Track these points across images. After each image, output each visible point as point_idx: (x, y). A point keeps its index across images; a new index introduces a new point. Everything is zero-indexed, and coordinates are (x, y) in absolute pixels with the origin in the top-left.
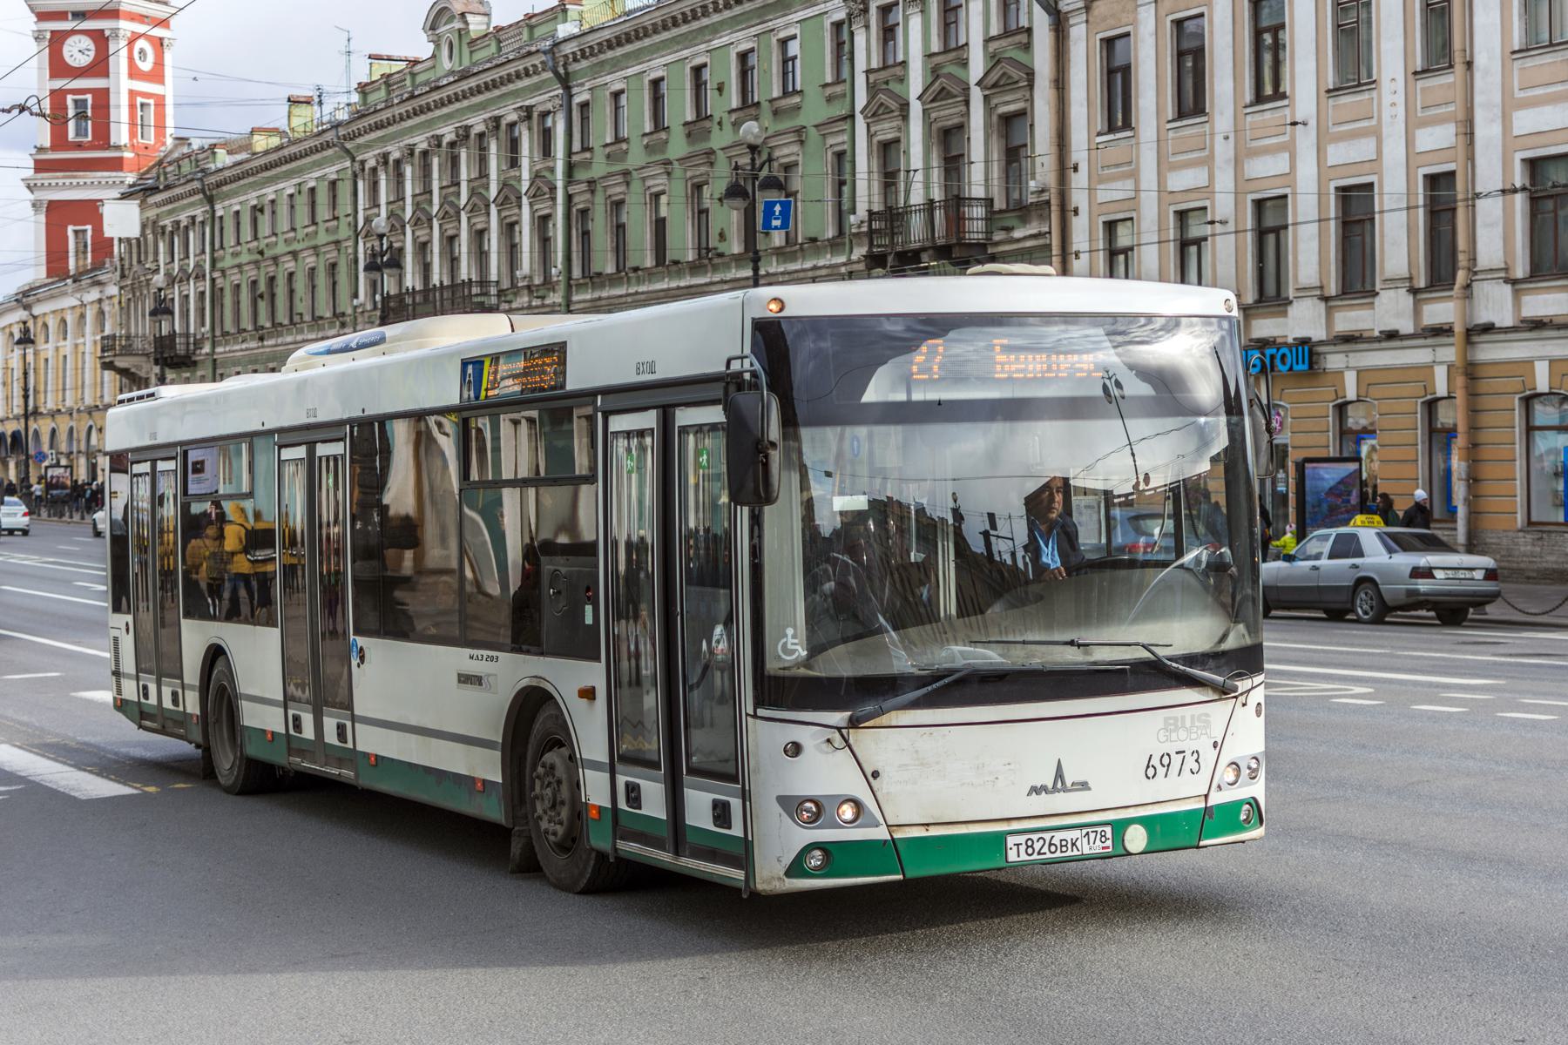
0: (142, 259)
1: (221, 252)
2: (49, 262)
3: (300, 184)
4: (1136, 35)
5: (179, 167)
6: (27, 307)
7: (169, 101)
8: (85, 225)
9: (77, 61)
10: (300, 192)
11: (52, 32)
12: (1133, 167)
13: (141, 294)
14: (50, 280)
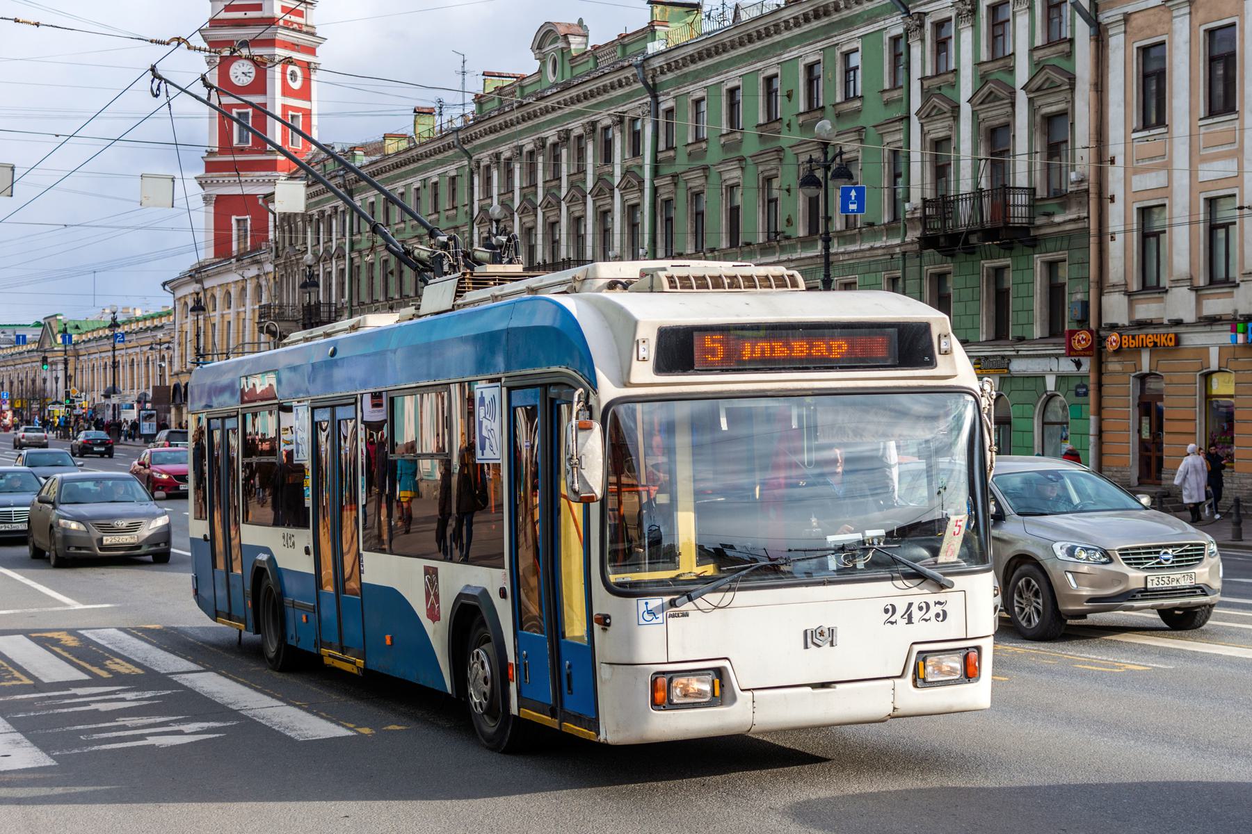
0: (293, 242)
1: (358, 237)
2: (216, 245)
3: (425, 180)
4: (1171, 43)
5: (325, 166)
6: (199, 281)
7: (314, 111)
9: (241, 81)
10: (425, 187)
12: (1166, 159)
13: (292, 271)
14: (217, 260)
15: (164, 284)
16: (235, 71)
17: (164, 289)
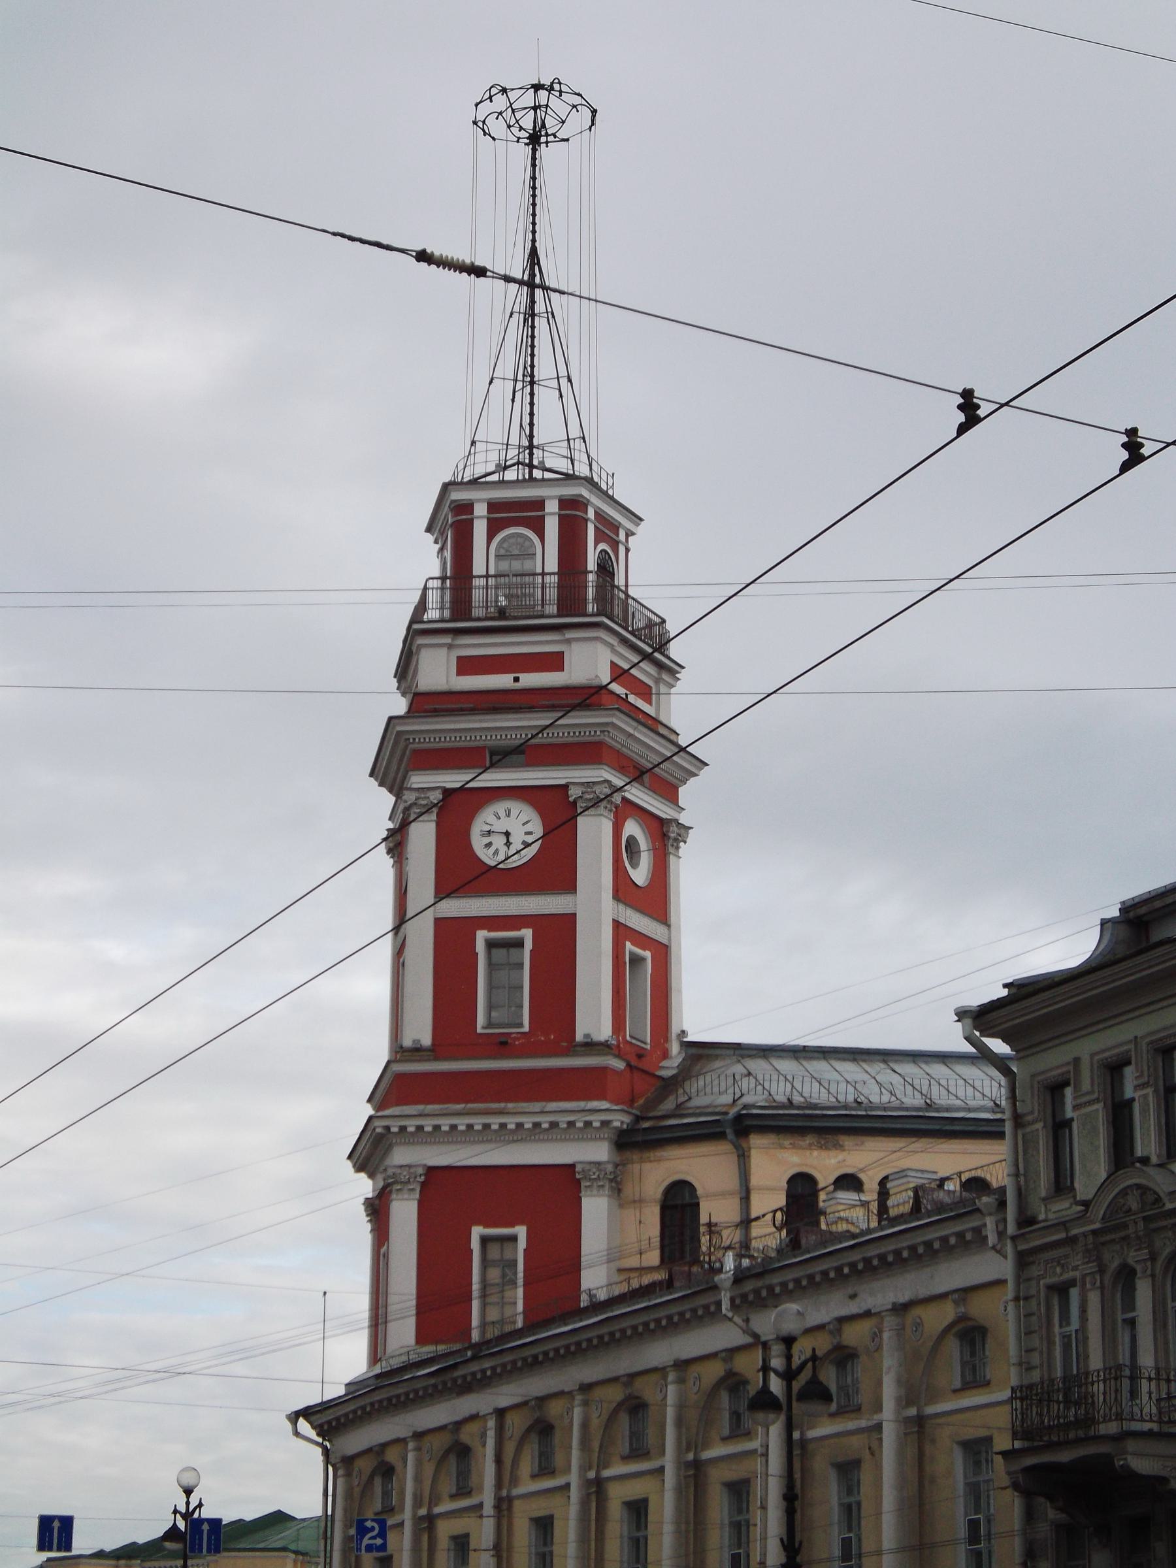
2: (419, 1314)
8: (512, 1225)
14: (428, 1350)
15: (294, 1417)
17: (297, 1433)
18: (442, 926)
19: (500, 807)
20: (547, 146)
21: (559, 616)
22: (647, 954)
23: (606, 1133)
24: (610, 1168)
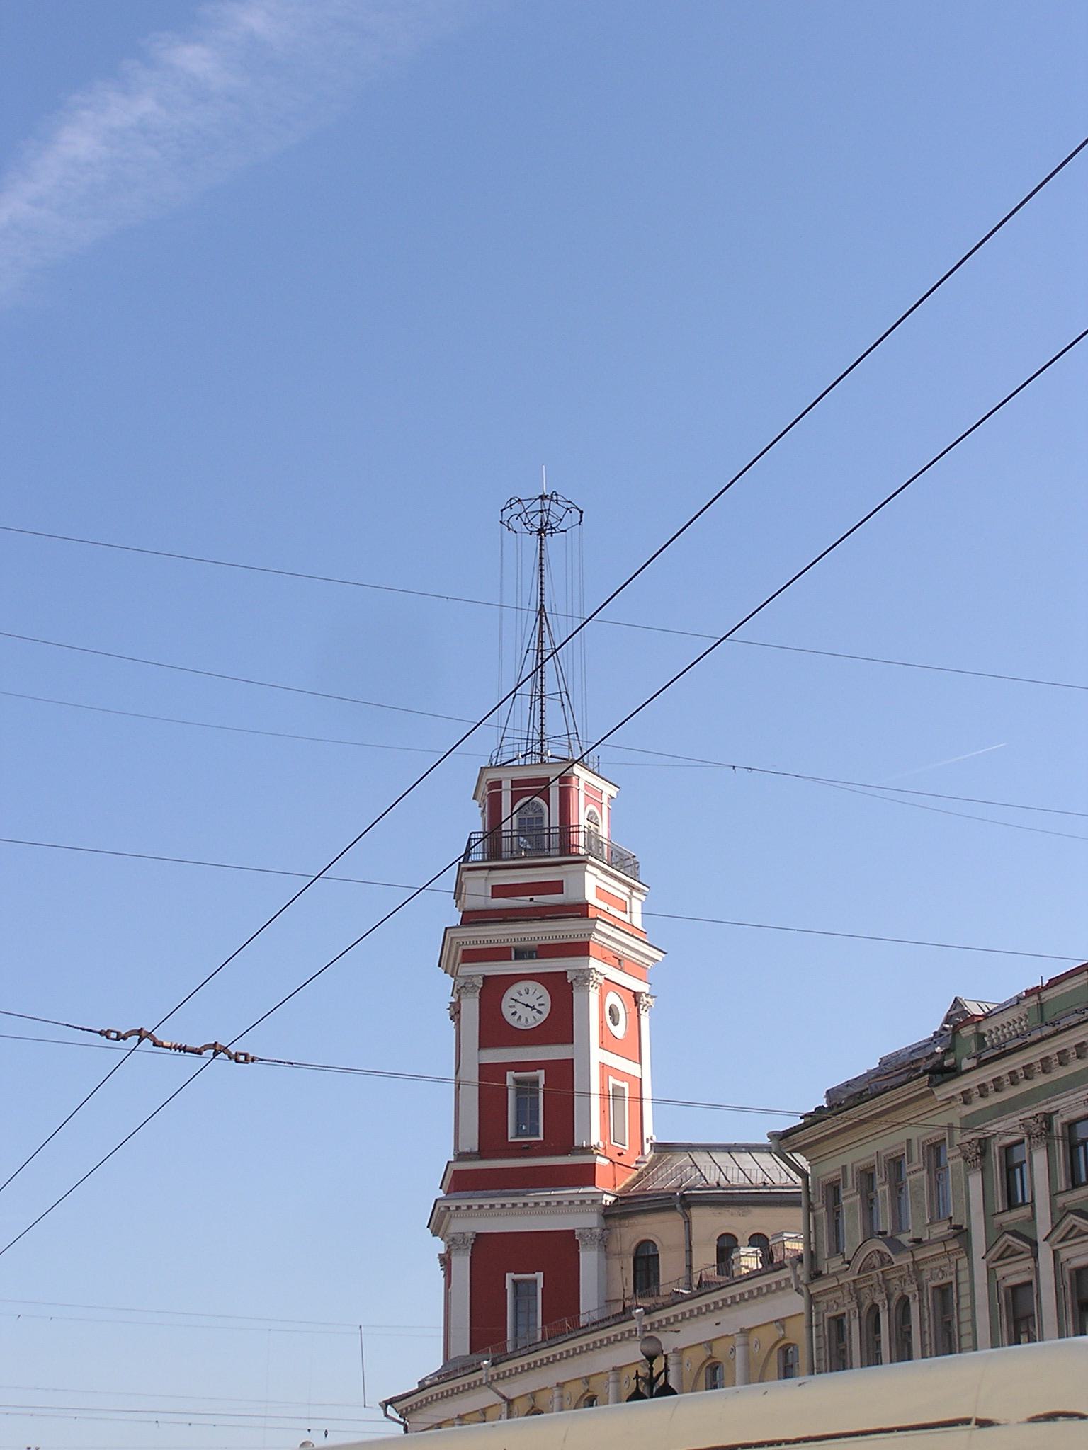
9: (523, 1019)
11: (485, 978)
16: (531, 992)
17: (386, 1415)
18: (486, 1071)
19: (521, 986)
20: (552, 536)
21: (560, 856)
22: (625, 1085)
23: (595, 1208)
24: (598, 1230)
